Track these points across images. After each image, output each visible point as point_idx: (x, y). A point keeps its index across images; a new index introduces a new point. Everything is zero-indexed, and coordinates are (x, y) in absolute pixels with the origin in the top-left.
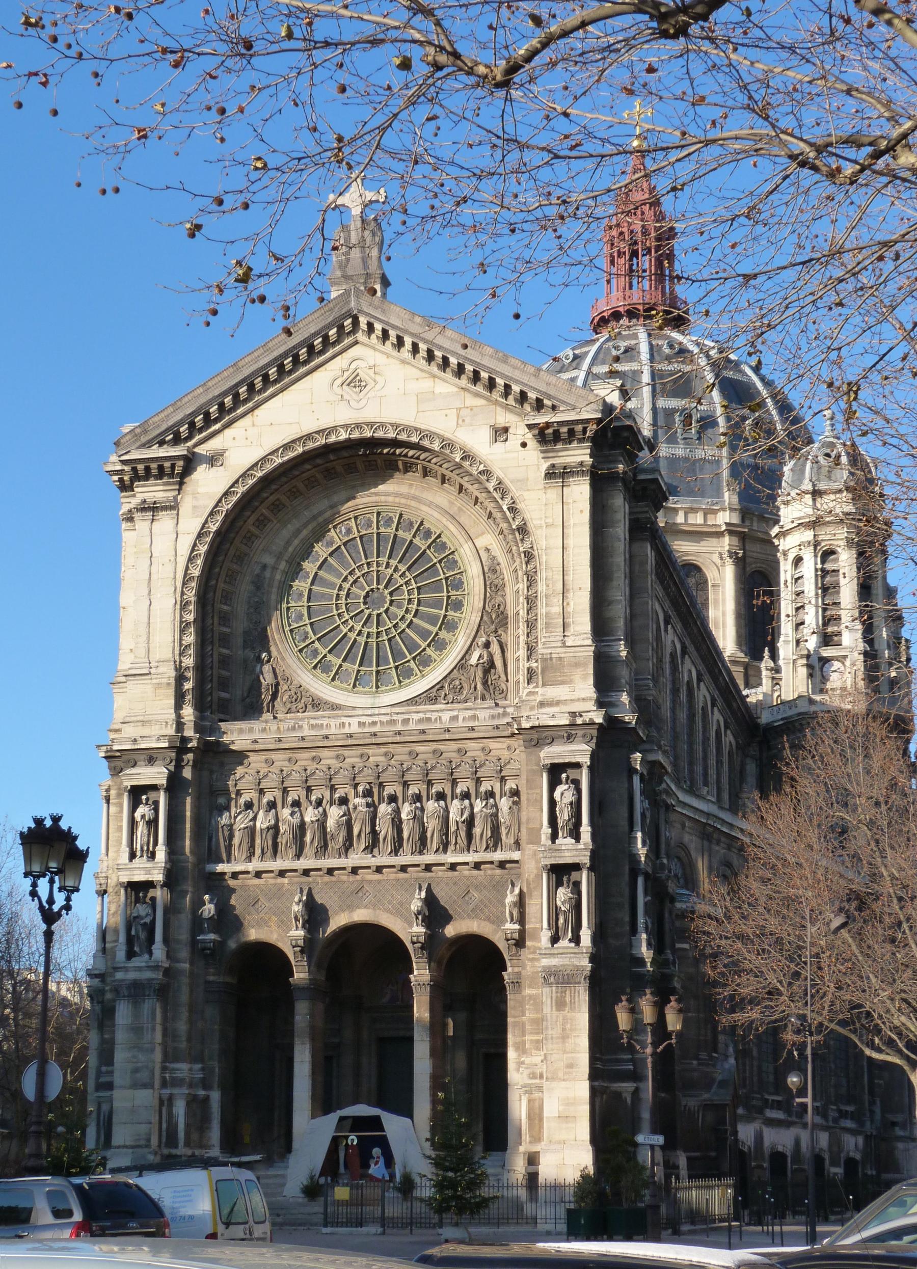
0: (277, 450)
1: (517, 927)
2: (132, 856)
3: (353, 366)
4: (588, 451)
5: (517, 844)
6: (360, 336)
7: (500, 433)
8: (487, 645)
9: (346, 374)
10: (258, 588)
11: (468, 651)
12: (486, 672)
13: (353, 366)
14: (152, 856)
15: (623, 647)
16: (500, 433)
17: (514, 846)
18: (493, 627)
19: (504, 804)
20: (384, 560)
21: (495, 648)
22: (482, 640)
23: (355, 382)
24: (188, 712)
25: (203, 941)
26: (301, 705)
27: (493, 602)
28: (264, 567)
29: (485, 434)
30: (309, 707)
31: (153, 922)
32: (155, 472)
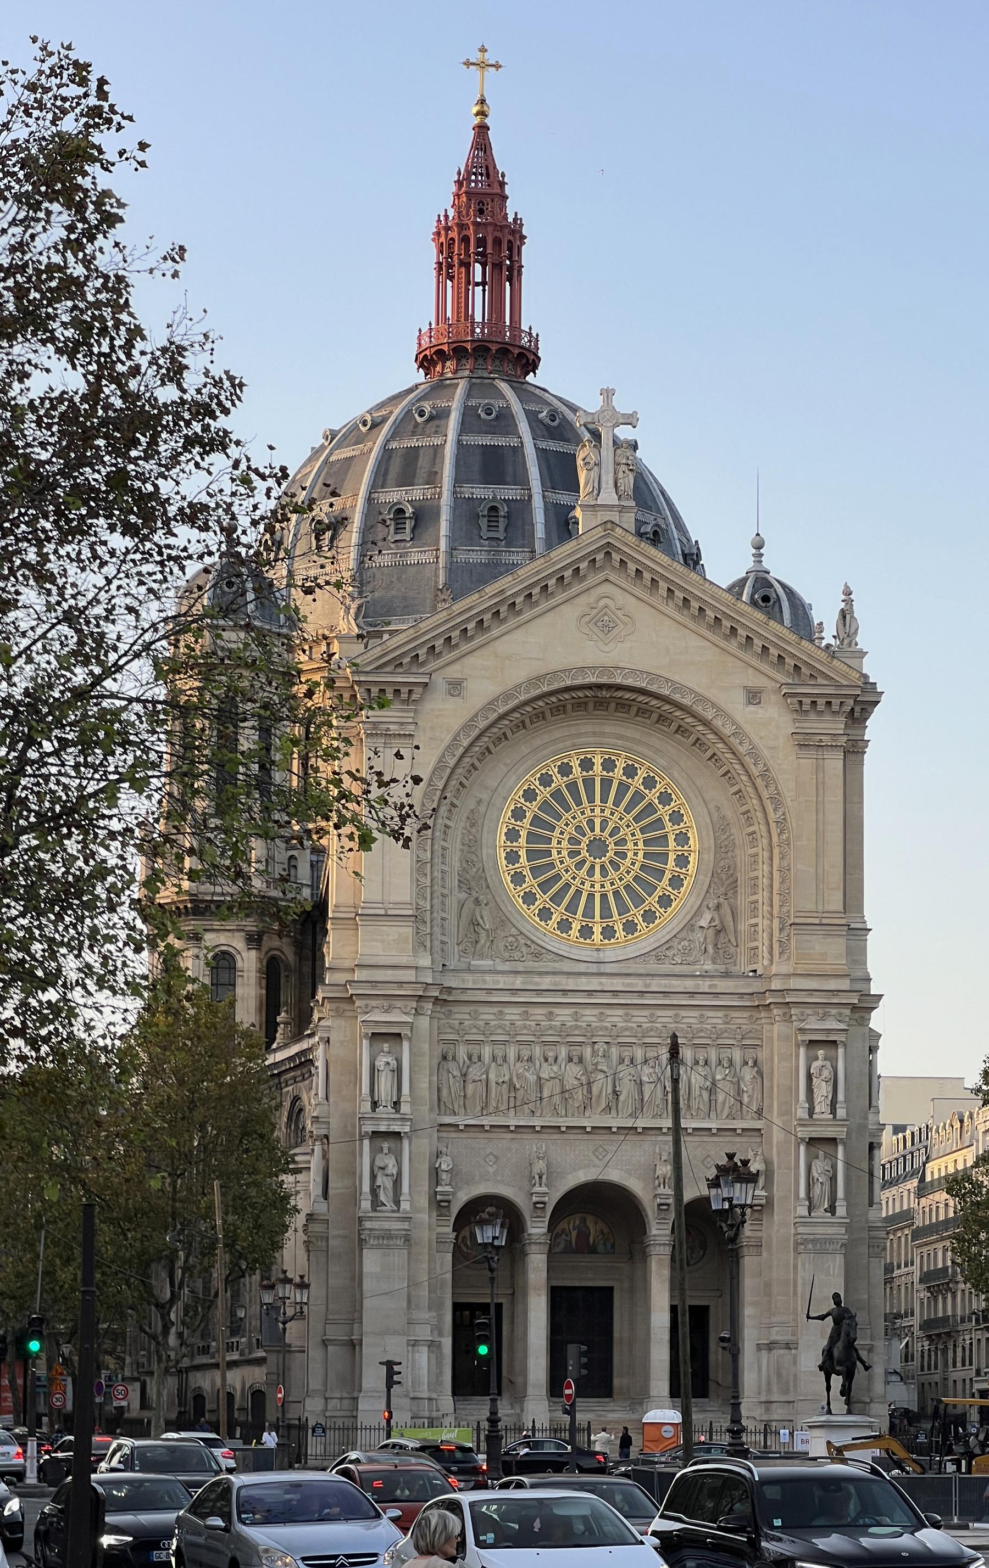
0: (520, 686)
1: (763, 1193)
2: (375, 1104)
5: (759, 1113)
7: (753, 696)
9: (595, 612)
10: (473, 825)
11: (698, 913)
14: (396, 1105)
16: (753, 696)
17: (756, 1116)
18: (722, 890)
19: (748, 1074)
21: (726, 909)
25: (442, 1193)
28: (479, 802)
29: (740, 696)
31: (399, 1174)
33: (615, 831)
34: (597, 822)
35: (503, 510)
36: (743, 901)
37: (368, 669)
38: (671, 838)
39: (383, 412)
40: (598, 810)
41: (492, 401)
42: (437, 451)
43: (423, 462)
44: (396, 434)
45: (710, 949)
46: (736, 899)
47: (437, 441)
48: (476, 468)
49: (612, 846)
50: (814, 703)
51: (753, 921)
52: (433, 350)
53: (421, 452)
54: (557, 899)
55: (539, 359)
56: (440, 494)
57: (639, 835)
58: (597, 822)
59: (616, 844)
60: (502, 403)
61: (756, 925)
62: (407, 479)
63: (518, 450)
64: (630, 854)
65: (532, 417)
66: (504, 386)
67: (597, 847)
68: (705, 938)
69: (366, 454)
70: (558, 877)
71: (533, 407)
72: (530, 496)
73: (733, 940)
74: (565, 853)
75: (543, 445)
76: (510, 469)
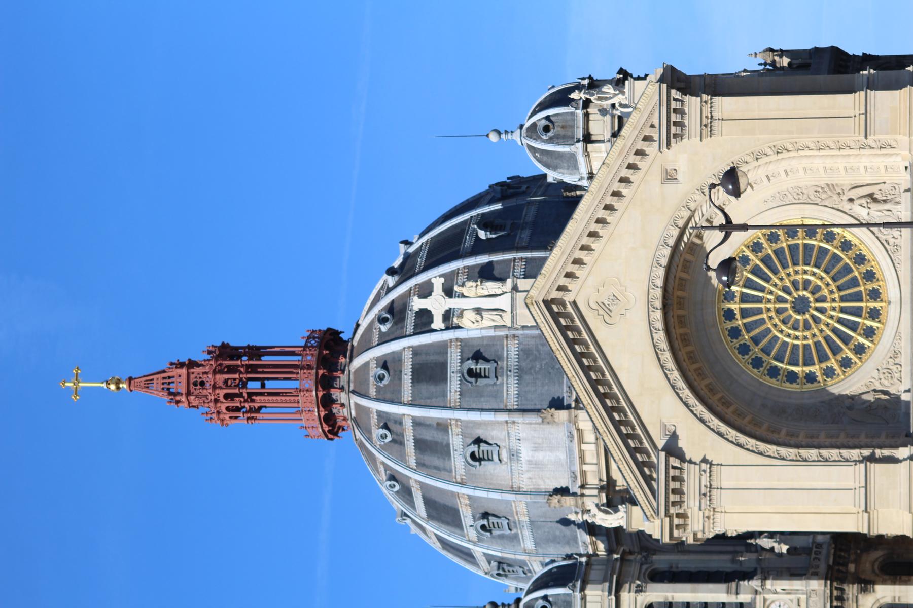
3: (595, 306)
4: (694, 98)
6: (568, 298)
7: (669, 177)
8: (851, 200)
9: (601, 312)
12: (875, 200)
13: (595, 306)
15: (865, 73)
16: (669, 177)
18: (835, 197)
20: (775, 280)
22: (846, 206)
23: (605, 309)
24: (903, 452)
26: (894, 368)
27: (812, 197)
29: (670, 187)
30: (897, 361)
32: (677, 485)
33: (785, 290)
34: (778, 305)
35: (471, 364)
36: (845, 180)
37: (655, 504)
38: (792, 242)
39: (382, 469)
40: (769, 306)
41: (372, 374)
42: (418, 423)
43: (428, 435)
44: (402, 458)
45: (887, 206)
46: (842, 185)
47: (408, 424)
48: (432, 388)
49: (801, 293)
50: (675, 124)
51: (862, 170)
52: (324, 425)
53: (418, 437)
54: (846, 339)
55: (329, 329)
56: (457, 420)
57: (791, 270)
58: (778, 305)
59: (797, 289)
60: (373, 365)
61: (866, 168)
62: (444, 450)
63: (417, 351)
64: (806, 277)
65: (384, 339)
66: (358, 362)
67: (801, 306)
68: (879, 211)
69: (423, 486)
70: (827, 339)
71: (376, 340)
72: (457, 340)
73: (879, 187)
74: (807, 333)
75: (410, 329)
76: (433, 358)
